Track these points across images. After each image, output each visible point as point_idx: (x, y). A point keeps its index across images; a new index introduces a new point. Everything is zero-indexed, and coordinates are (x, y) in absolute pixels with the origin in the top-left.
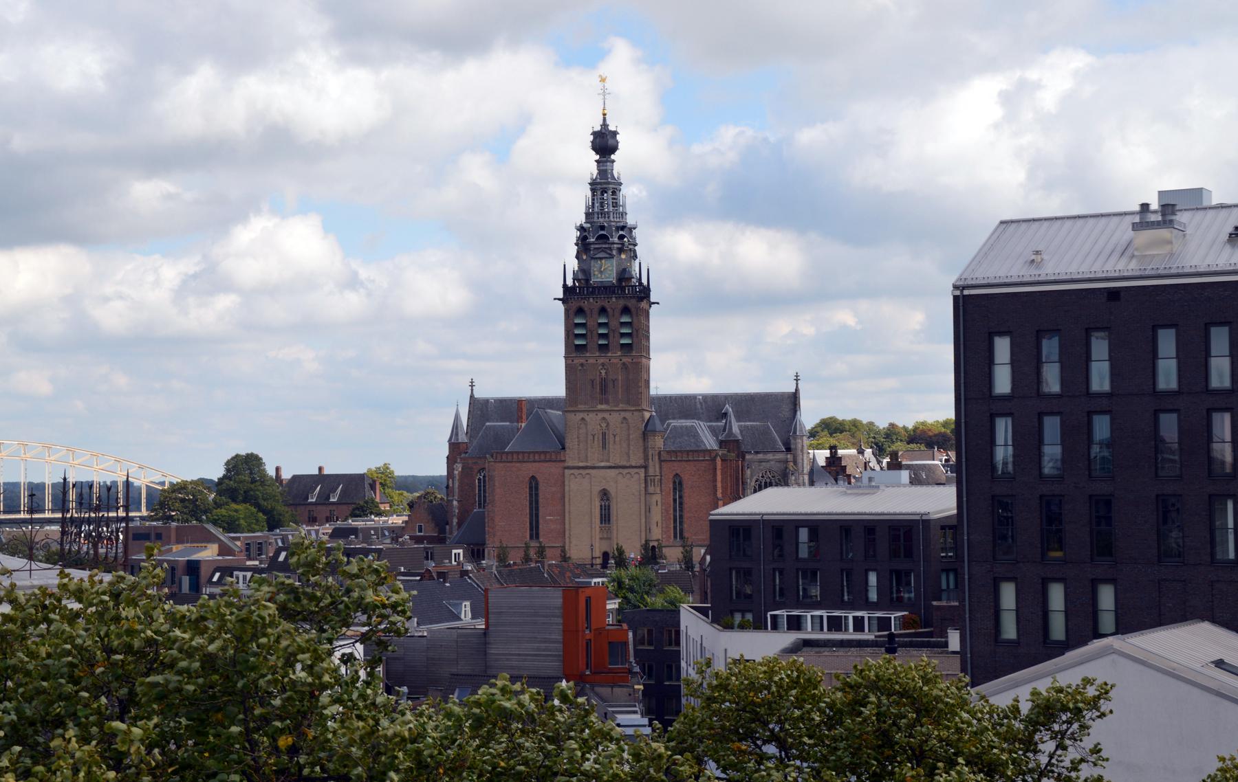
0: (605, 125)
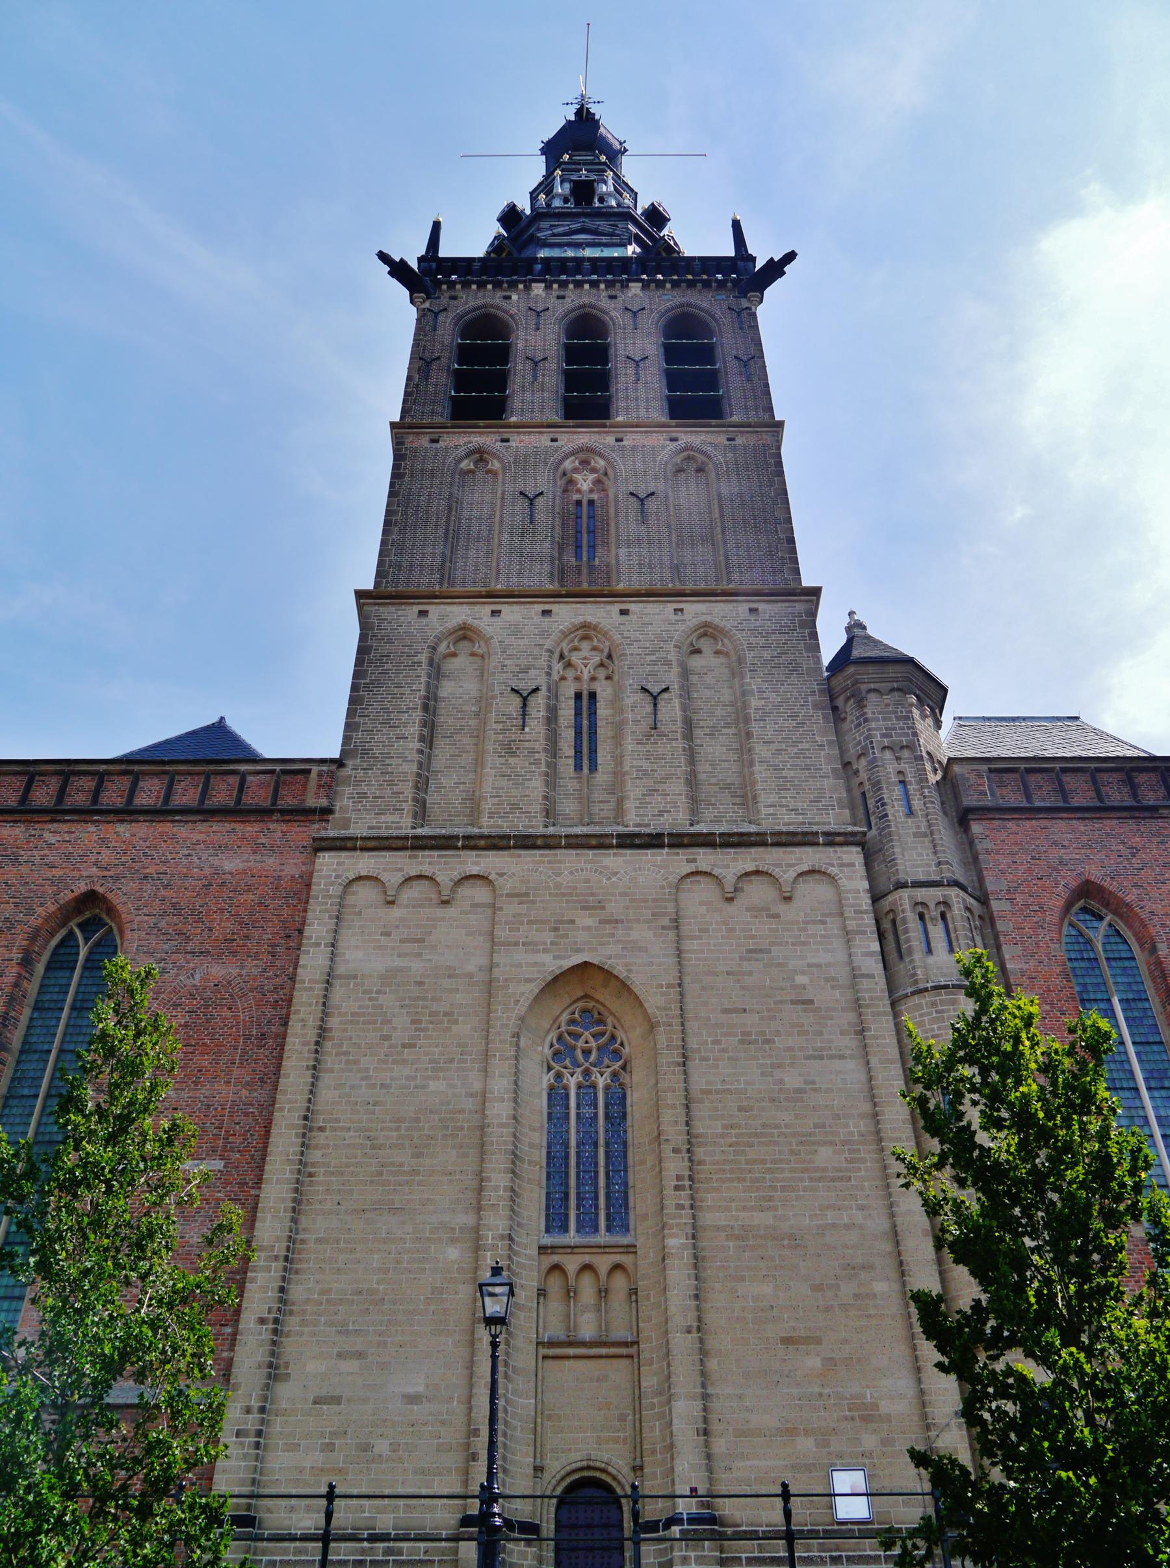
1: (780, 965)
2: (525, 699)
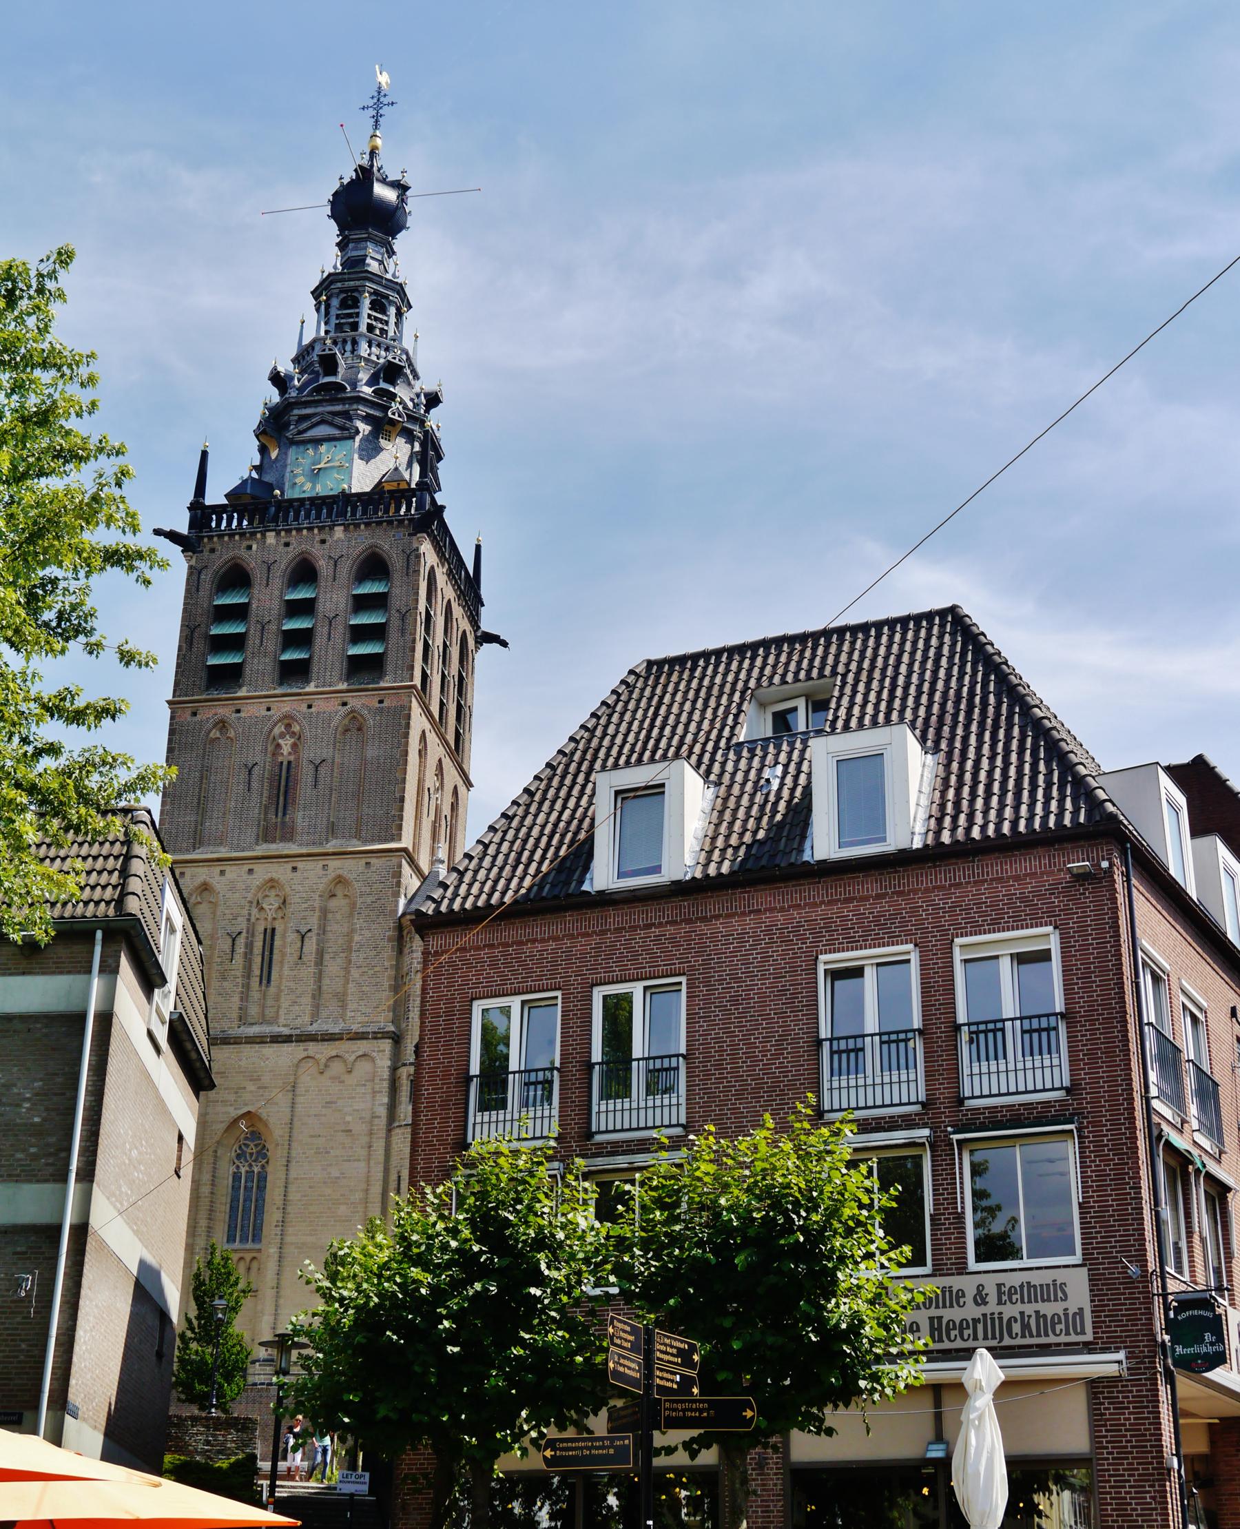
1: (340, 1111)
2: (234, 940)
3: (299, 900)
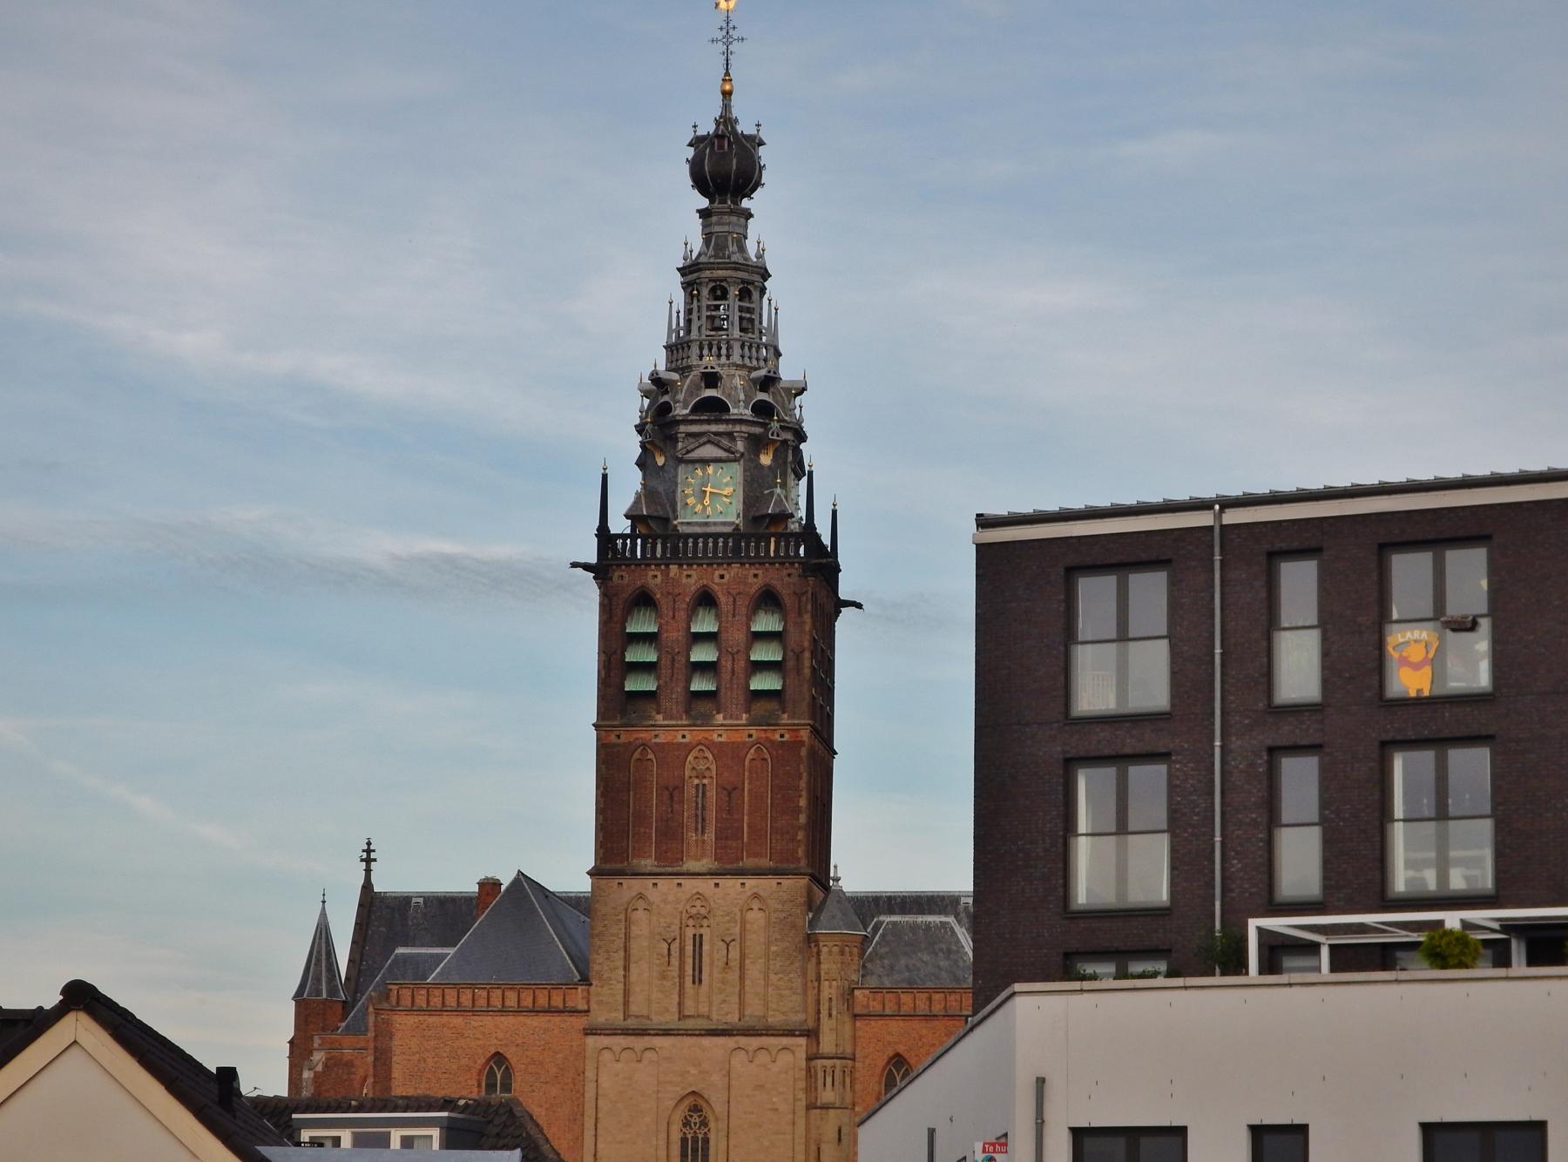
0: (726, 120)
3: (722, 913)
